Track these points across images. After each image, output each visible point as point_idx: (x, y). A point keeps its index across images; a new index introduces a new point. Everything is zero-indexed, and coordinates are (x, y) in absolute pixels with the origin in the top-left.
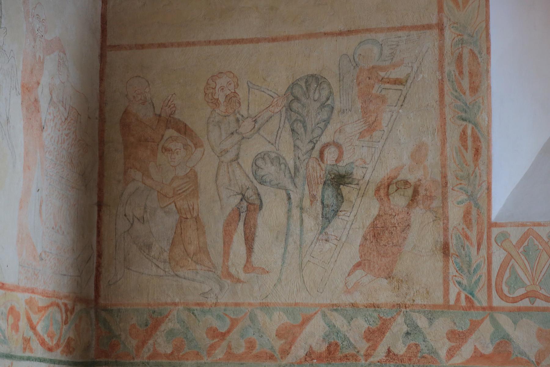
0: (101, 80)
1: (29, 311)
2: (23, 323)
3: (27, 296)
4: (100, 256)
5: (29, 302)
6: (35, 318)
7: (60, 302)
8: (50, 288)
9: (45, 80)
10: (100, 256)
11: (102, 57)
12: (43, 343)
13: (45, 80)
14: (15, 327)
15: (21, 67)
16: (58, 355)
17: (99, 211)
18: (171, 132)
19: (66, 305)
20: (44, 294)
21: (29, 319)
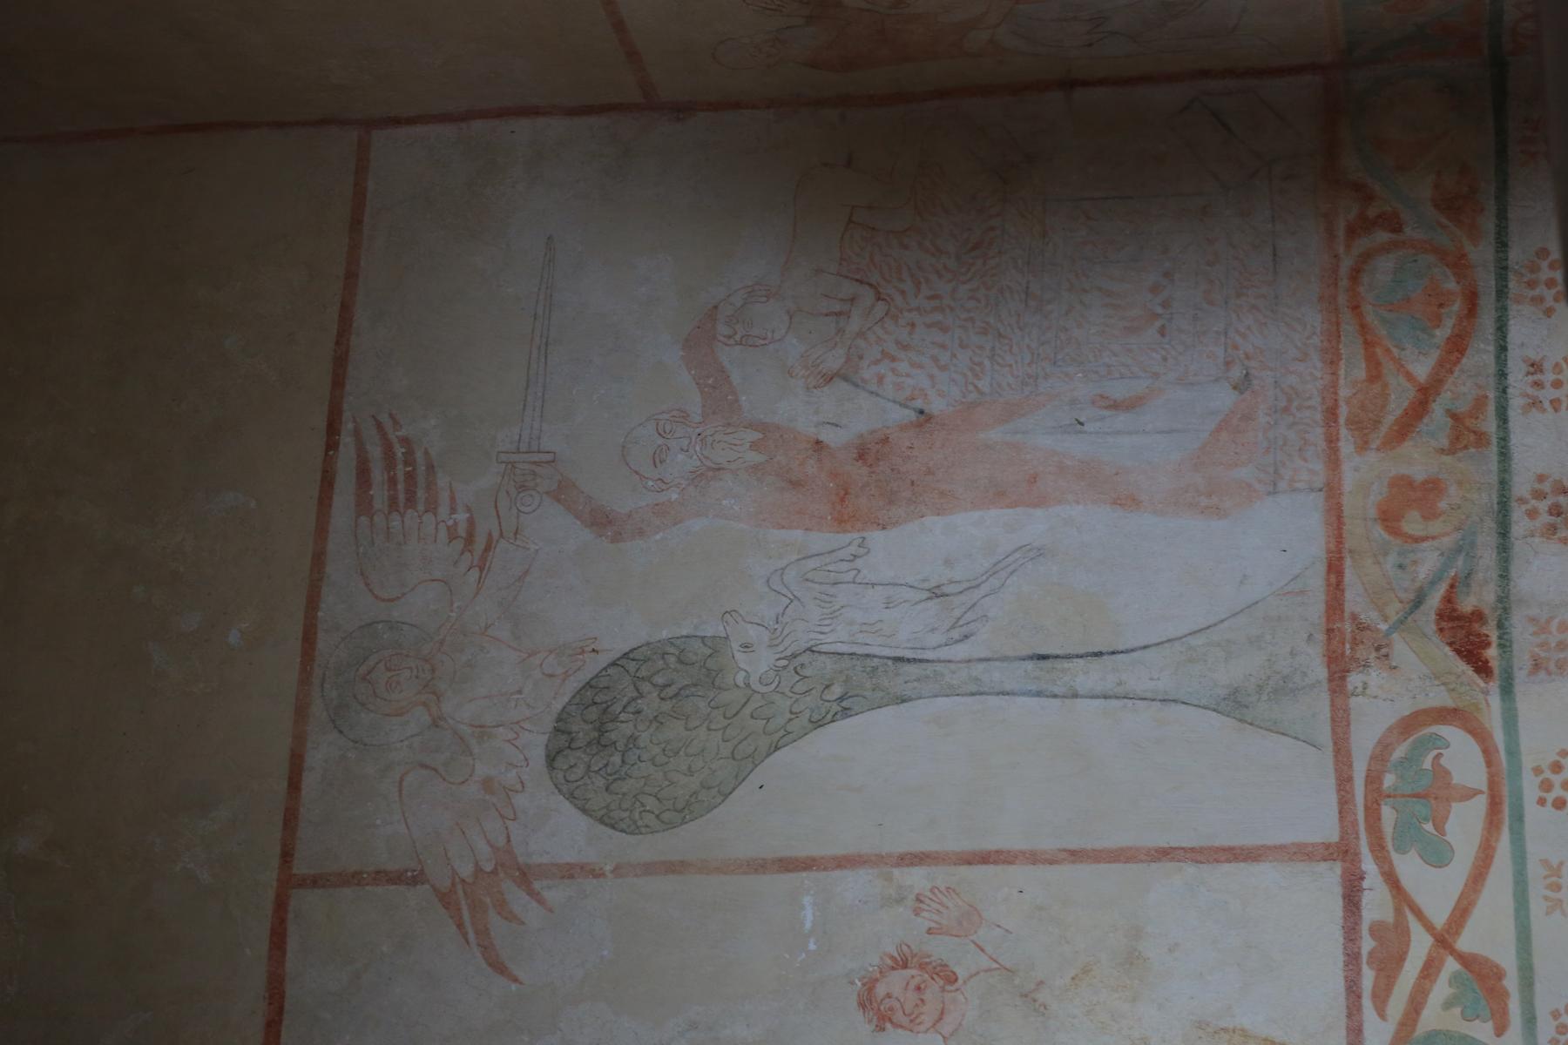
0: (737, 106)
1: (1384, 429)
3: (1346, 447)
4: (1205, 74)
5: (1363, 427)
6: (1399, 398)
7: (1346, 264)
8: (1314, 319)
9: (804, 411)
10: (1205, 74)
11: (681, 110)
12: (1457, 346)
13: (804, 411)
15: (797, 535)
16: (1481, 253)
17: (1085, 83)
19: (1352, 232)
20: (1332, 360)
21: (1405, 428)
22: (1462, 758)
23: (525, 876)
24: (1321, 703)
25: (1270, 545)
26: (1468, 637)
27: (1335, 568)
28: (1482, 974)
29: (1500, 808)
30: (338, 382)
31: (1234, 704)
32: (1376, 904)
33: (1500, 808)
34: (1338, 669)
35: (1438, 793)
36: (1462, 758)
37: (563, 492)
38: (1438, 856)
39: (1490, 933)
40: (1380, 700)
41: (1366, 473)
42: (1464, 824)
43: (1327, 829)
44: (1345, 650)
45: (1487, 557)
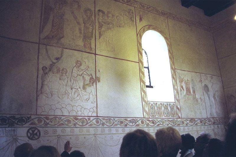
2: (218, 121)
6: (220, 120)
11: (224, 90)
14: (217, 121)
18: (232, 97)
22: (211, 123)
23: (202, 83)
24: (211, 117)
25: (215, 115)
26: (214, 123)
27: (215, 118)
28: (205, 124)
29: (210, 124)
30: (214, 75)
31: (211, 113)
32: (206, 119)
33: (210, 124)
34: (212, 118)
35: (210, 122)
36: (211, 123)
37: (212, 85)
38: (208, 122)
39: (206, 124)
40: (211, 119)
41: (218, 119)
42: (209, 123)
43: (208, 117)
44: (213, 118)
45: (216, 124)
